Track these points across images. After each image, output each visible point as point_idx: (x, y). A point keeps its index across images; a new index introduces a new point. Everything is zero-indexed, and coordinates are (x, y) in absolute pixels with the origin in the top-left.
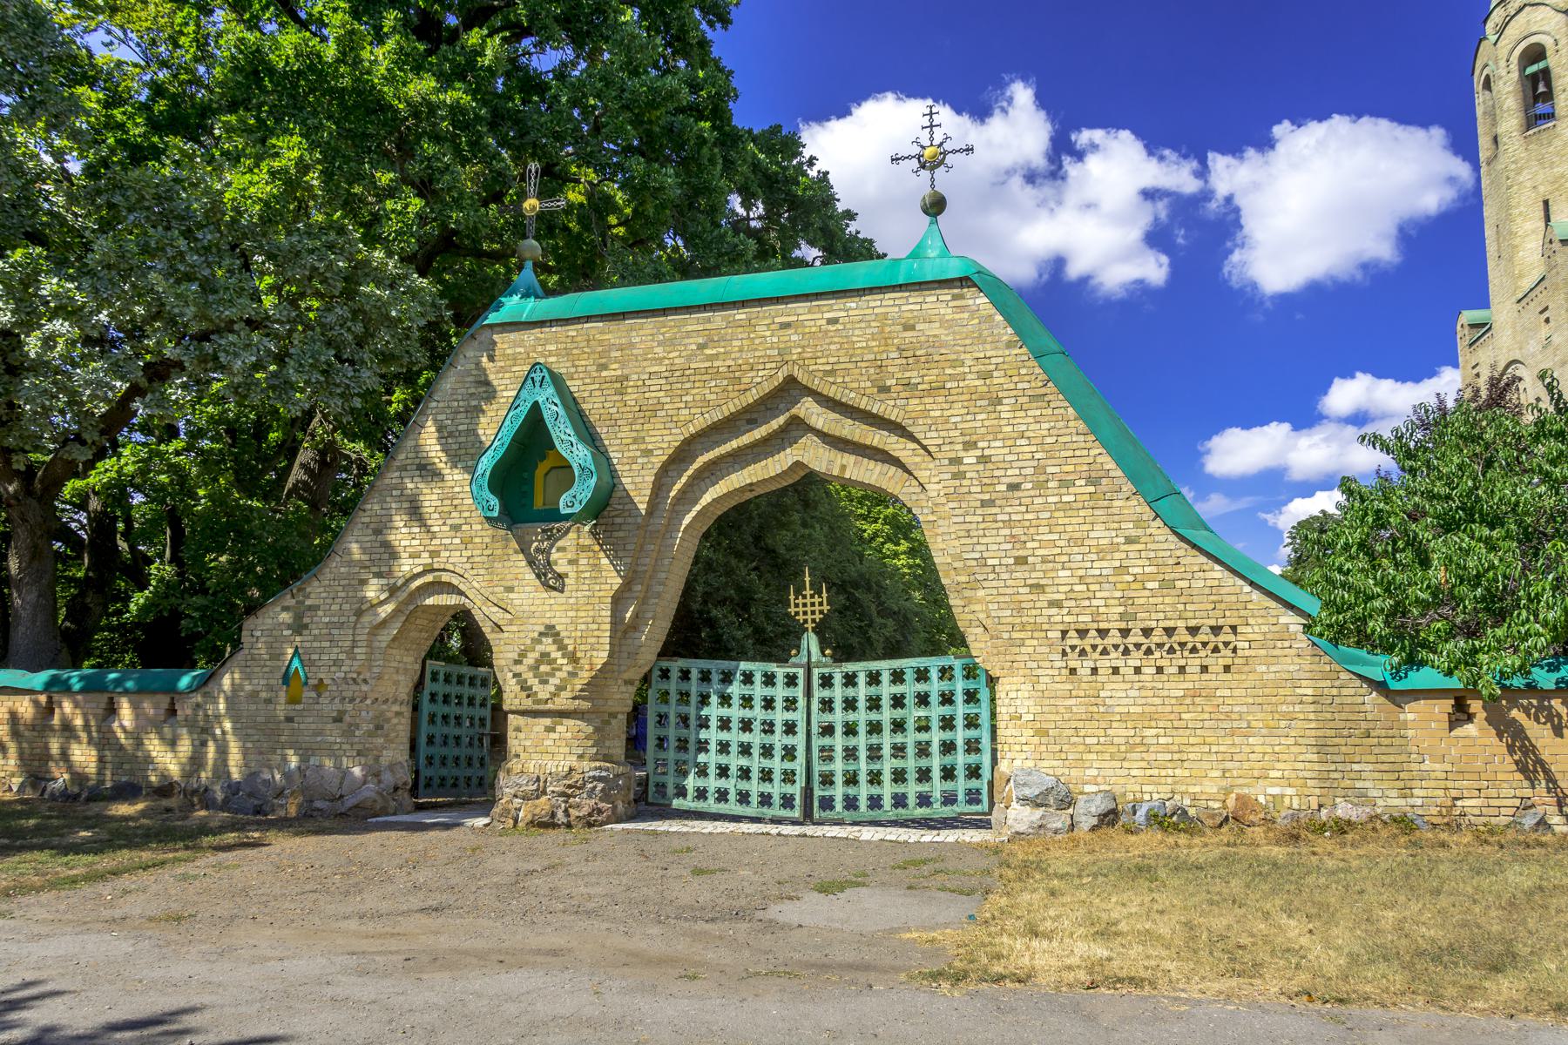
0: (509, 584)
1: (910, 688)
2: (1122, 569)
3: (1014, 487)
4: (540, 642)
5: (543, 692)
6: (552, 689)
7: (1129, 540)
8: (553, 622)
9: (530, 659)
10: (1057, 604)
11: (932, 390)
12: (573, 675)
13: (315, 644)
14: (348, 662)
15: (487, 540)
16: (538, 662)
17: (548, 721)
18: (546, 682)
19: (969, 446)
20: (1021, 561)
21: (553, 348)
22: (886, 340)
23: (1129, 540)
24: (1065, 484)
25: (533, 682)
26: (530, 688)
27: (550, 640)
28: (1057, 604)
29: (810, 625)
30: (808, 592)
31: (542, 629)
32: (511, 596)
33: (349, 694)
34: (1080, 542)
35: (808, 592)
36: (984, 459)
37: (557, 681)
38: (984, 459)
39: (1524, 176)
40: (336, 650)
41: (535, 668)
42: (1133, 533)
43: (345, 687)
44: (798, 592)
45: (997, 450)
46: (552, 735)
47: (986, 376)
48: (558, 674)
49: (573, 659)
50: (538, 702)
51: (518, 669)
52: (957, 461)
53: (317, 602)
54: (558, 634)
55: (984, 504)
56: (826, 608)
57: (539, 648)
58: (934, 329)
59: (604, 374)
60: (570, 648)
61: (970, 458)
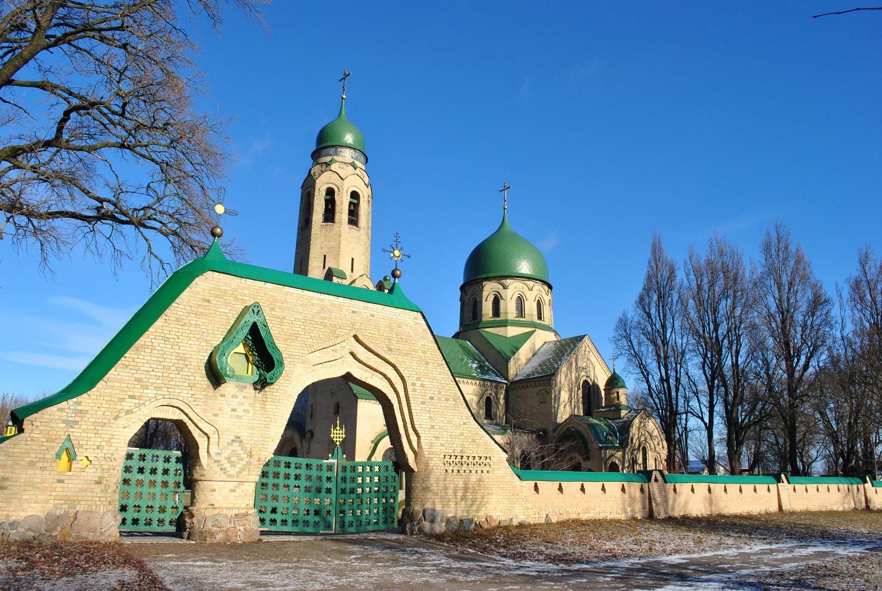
0: (216, 412)
1: (292, 471)
2: (461, 434)
3: (432, 398)
4: (232, 445)
5: (233, 471)
6: (238, 470)
7: (464, 424)
8: (240, 435)
9: (226, 454)
10: (442, 445)
11: (406, 355)
12: (249, 463)
13: (83, 435)
14: (107, 448)
15: (205, 387)
16: (238, 456)
17: (232, 485)
18: (235, 466)
19: (418, 379)
20: (433, 427)
21: (247, 292)
22: (391, 329)
23: (464, 424)
24: (447, 400)
25: (227, 465)
26: (225, 469)
27: (238, 444)
28: (442, 445)
29: (338, 443)
30: (338, 428)
31: (233, 438)
32: (217, 418)
33: (107, 467)
34: (449, 422)
35: (338, 428)
36: (422, 386)
37: (241, 466)
38: (422, 386)
39: (318, 241)
40: (99, 439)
41: (228, 459)
42: (465, 421)
43: (104, 463)
44: (335, 428)
45: (427, 383)
46: (234, 494)
47: (424, 352)
48: (241, 462)
49: (250, 455)
50: (230, 476)
51: (219, 458)
52: (413, 384)
53: (86, 408)
54: (242, 441)
55: (423, 403)
56: (344, 436)
57: (231, 448)
58: (408, 329)
59: (273, 313)
60: (249, 449)
61: (418, 384)
